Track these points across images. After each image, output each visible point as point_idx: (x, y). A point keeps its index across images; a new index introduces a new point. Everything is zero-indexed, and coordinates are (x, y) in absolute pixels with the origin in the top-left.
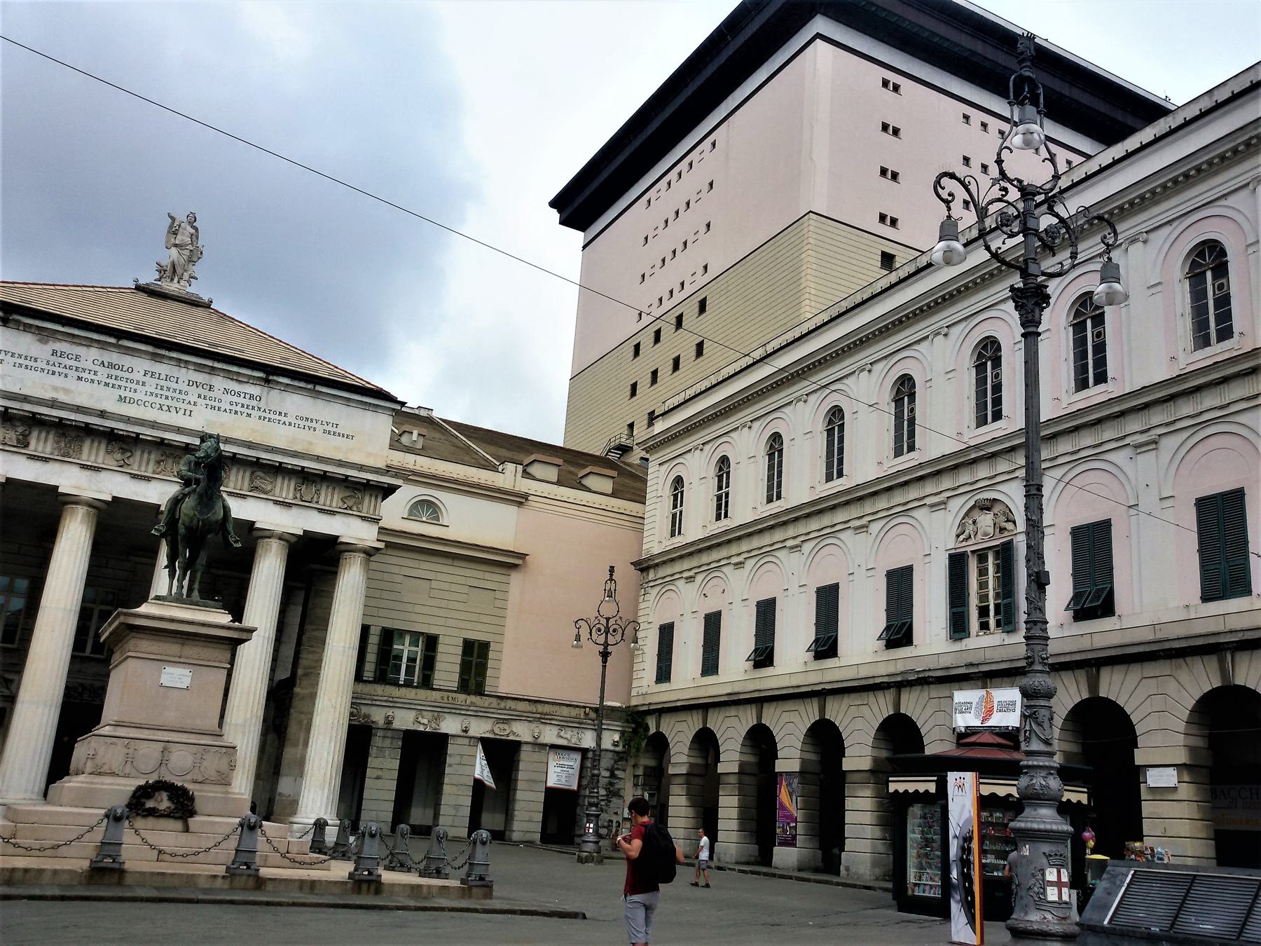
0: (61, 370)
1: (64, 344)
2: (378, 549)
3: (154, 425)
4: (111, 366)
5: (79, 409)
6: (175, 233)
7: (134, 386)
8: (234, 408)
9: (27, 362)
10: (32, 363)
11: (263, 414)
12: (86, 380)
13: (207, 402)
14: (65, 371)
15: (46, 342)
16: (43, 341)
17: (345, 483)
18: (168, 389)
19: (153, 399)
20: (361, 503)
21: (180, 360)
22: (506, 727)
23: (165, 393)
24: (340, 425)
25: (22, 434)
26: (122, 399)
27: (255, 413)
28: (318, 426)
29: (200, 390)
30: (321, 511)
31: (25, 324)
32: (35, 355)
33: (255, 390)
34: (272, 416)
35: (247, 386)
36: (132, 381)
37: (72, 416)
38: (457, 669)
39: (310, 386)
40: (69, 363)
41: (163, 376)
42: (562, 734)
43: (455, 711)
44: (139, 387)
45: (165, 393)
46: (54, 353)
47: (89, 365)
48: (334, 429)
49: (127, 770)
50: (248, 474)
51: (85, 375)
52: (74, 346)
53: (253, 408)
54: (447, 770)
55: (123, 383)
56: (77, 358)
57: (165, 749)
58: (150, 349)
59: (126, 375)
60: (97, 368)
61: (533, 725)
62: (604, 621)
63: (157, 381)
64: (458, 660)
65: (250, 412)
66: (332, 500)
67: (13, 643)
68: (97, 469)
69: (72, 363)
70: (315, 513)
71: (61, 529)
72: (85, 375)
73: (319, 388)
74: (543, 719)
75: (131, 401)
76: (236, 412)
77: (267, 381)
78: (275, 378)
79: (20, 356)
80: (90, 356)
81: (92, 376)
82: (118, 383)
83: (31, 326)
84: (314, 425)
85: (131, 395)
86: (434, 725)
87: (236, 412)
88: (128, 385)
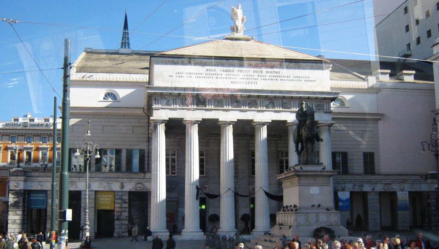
2: (333, 124)
7: (235, 77)
8: (271, 78)
9: (199, 76)
10: (202, 76)
12: (219, 78)
13: (261, 77)
19: (242, 80)
22: (389, 186)
23: (246, 77)
27: (279, 78)
34: (285, 78)
38: (362, 165)
40: (213, 73)
42: (413, 186)
43: (369, 182)
46: (207, 70)
47: (219, 72)
48: (308, 79)
49: (307, 224)
50: (281, 102)
51: (218, 76)
53: (278, 77)
54: (369, 205)
55: (231, 77)
56: (215, 70)
57: (317, 215)
59: (232, 73)
60: (221, 73)
61: (400, 184)
62: (434, 142)
64: (362, 161)
67: (203, 174)
72: (218, 76)
74: (404, 181)
75: (235, 82)
76: (272, 80)
81: (221, 76)
82: (230, 77)
84: (300, 79)
86: (360, 188)
87: (272, 80)
88: (234, 77)
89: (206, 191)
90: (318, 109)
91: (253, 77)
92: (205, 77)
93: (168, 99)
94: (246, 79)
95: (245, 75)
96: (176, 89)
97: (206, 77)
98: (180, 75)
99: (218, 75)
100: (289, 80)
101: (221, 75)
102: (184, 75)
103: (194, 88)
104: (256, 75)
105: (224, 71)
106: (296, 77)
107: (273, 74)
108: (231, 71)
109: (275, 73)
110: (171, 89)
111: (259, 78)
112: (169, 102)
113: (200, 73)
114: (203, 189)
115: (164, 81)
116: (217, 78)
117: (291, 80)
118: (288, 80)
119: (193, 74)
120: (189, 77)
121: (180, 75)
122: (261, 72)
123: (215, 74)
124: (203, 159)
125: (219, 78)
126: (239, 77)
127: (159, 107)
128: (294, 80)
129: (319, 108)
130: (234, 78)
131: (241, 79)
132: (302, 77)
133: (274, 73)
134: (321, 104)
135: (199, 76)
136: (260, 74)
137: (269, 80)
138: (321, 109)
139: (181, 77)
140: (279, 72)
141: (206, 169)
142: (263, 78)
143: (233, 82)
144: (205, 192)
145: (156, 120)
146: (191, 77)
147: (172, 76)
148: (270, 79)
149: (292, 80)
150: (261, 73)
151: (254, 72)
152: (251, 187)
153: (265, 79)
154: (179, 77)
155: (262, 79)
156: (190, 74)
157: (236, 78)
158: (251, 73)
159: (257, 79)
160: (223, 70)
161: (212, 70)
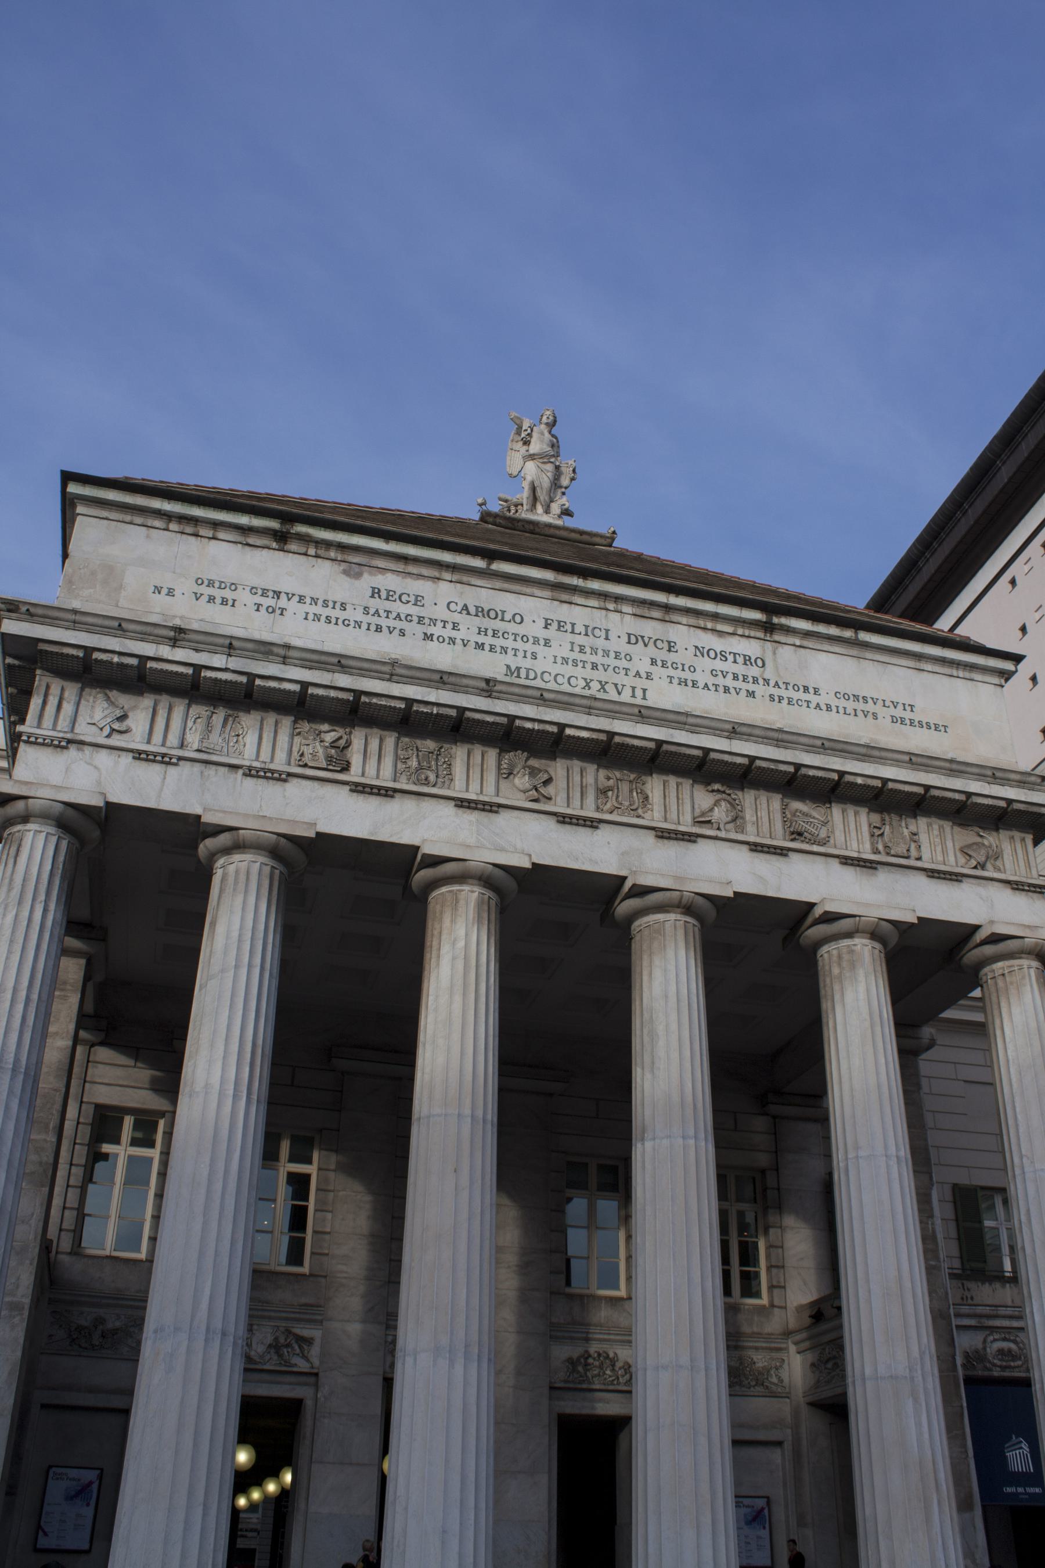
0: (392, 623)
1: (389, 575)
3: (590, 705)
4: (480, 612)
5: (442, 679)
6: (527, 443)
7: (529, 647)
10: (337, 613)
12: (441, 640)
13: (671, 672)
14: (398, 624)
15: (358, 576)
16: (353, 573)
17: (963, 812)
18: (594, 651)
20: (997, 856)
21: (604, 596)
24: (919, 705)
25: (333, 745)
27: (760, 689)
28: (878, 709)
30: (933, 874)
31: (319, 543)
32: (339, 598)
33: (751, 648)
35: (735, 640)
36: (525, 638)
37: (432, 695)
39: (848, 634)
44: (540, 649)
46: (375, 592)
48: (908, 715)
51: (437, 630)
52: (409, 581)
53: (755, 680)
58: (549, 575)
59: (512, 628)
60: (457, 617)
63: (570, 637)
65: (751, 687)
66: (944, 852)
68: (491, 808)
69: (410, 609)
70: (921, 881)
71: (431, 941)
73: (864, 636)
77: (769, 628)
78: (783, 620)
79: (314, 601)
80: (441, 595)
81: (448, 632)
82: (499, 642)
83: (328, 544)
84: (870, 707)
85: (528, 663)
87: (727, 690)
88: (519, 645)
89: (308, 1360)
90: (974, 863)
91: (623, 663)
92: (358, 624)
93: (124, 700)
94: (589, 666)
95: (582, 650)
96: (178, 636)
98: (218, 594)
99: (433, 622)
100: (813, 705)
101: (450, 626)
102: (244, 597)
103: (288, 647)
105: (468, 613)
106: (846, 697)
107: (728, 666)
108: (508, 617)
109: (740, 660)
110: (148, 631)
111: (657, 671)
112: (129, 722)
113: (330, 598)
114: (288, 1345)
115: (117, 606)
117: (824, 707)
118: (808, 702)
119: (296, 598)
120: (271, 610)
121: (218, 594)
122: (671, 647)
123: (420, 620)
124: (307, 1177)
125: (441, 640)
127: (61, 735)
128: (841, 710)
129: (982, 859)
130: (521, 654)
133: (735, 662)
134: (986, 843)
136: (661, 655)
137: (713, 688)
138: (989, 866)
139: (224, 602)
141: (315, 1232)
143: (518, 669)
144: (302, 1365)
145: (20, 805)
146: (283, 610)
147: (170, 592)
148: (716, 686)
150: (669, 651)
151: (629, 642)
152: (562, 1352)
153: (690, 684)
154: (211, 599)
155: (675, 681)
156: (277, 594)
157: (534, 656)
158: (619, 644)
159: (649, 676)
160: (465, 607)
161: (404, 598)
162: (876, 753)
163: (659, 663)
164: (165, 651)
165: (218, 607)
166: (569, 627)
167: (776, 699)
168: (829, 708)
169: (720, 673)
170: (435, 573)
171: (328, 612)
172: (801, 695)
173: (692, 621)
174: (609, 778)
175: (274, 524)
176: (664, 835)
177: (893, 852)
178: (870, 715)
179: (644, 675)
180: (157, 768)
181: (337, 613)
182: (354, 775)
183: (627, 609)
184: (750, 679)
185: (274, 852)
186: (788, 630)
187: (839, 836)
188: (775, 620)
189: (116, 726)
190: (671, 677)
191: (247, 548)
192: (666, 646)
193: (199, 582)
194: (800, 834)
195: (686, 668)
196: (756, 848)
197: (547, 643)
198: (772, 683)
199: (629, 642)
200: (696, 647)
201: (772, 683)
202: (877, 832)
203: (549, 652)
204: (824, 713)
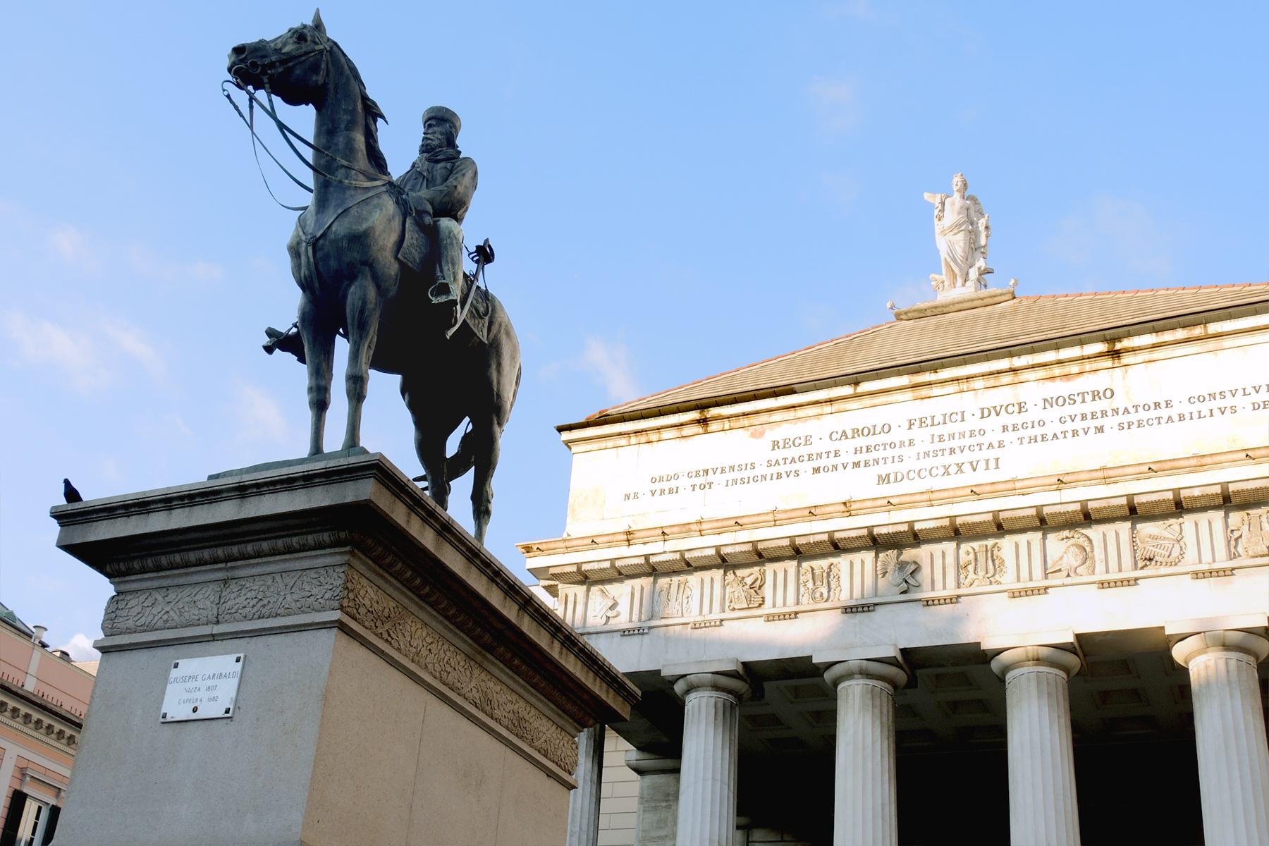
0: (789, 467)
1: (785, 425)
4: (856, 432)
7: (897, 452)
8: (1070, 426)
10: (749, 473)
11: (1125, 419)
12: (826, 470)
13: (1022, 433)
14: (793, 467)
15: (762, 434)
18: (952, 436)
23: (947, 445)
26: (884, 479)
27: (1110, 422)
28: (1239, 401)
29: (1005, 419)
34: (1143, 415)
39: (1198, 331)
41: (939, 419)
44: (906, 451)
45: (947, 445)
46: (775, 445)
53: (1104, 414)
55: (880, 454)
56: (808, 440)
58: (905, 380)
59: (884, 438)
65: (1098, 423)
73: (1213, 328)
76: (1075, 433)
77: (1115, 354)
78: (1126, 343)
79: (732, 468)
81: (833, 461)
84: (1229, 401)
87: (1075, 433)
88: (889, 453)
94: (947, 453)
95: (941, 439)
97: (769, 477)
98: (666, 486)
102: (684, 482)
104: (994, 422)
106: (1201, 399)
107: (1078, 409)
108: (878, 429)
109: (1088, 398)
111: (1010, 436)
116: (816, 470)
117: (1176, 418)
120: (703, 487)
121: (666, 486)
122: (1021, 407)
126: (921, 447)
128: (1195, 415)
131: (922, 455)
132: (1240, 392)
133: (1084, 401)
135: (736, 475)
139: (671, 491)
140: (1108, 394)
142: (1031, 432)
143: (888, 476)
146: (710, 484)
147: (636, 496)
148: (1065, 433)
149: (1182, 417)
151: (983, 417)
153: (1039, 438)
154: (662, 492)
155: (1026, 441)
156: (706, 472)
158: (974, 423)
159: (1001, 444)
162: (1208, 460)
163: (1010, 428)
164: (624, 551)
165: (667, 496)
166: (929, 422)
167: (1126, 426)
168: (1182, 417)
169: (1068, 419)
170: (816, 410)
171: (745, 474)
172: (1153, 414)
173: (1041, 373)
174: (968, 553)
175: (695, 415)
176: (1015, 594)
177: (1251, 553)
178: (1228, 411)
179: (996, 445)
180: (636, 639)
181: (749, 473)
182: (767, 609)
183: (978, 383)
184: (1099, 415)
185: (716, 687)
186: (1134, 350)
187: (1191, 554)
188: (1118, 346)
189: (610, 614)
190: (1021, 439)
191: (683, 441)
192: (1016, 408)
193: (653, 480)
194: (1150, 560)
195: (1036, 424)
196: (1103, 585)
197: (911, 443)
198: (1121, 411)
199: (983, 417)
200: (1045, 400)
201: (1121, 411)
202: (1236, 534)
203: (914, 450)
204: (1177, 424)
